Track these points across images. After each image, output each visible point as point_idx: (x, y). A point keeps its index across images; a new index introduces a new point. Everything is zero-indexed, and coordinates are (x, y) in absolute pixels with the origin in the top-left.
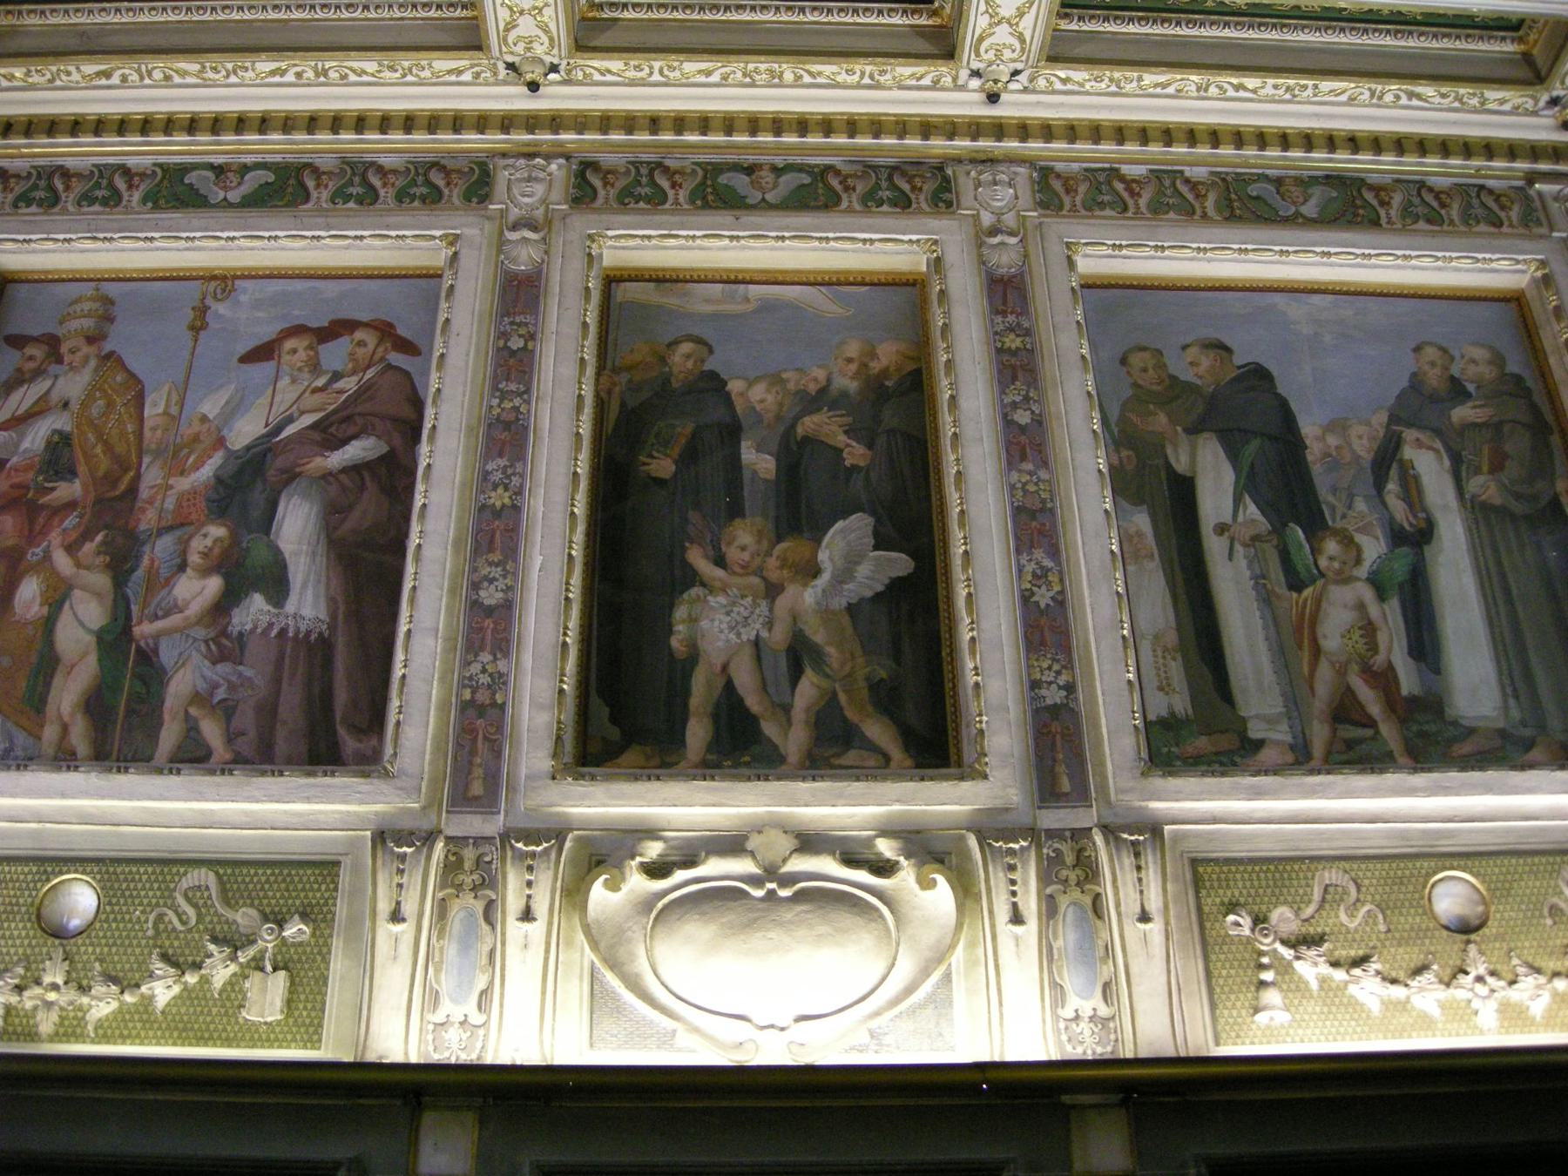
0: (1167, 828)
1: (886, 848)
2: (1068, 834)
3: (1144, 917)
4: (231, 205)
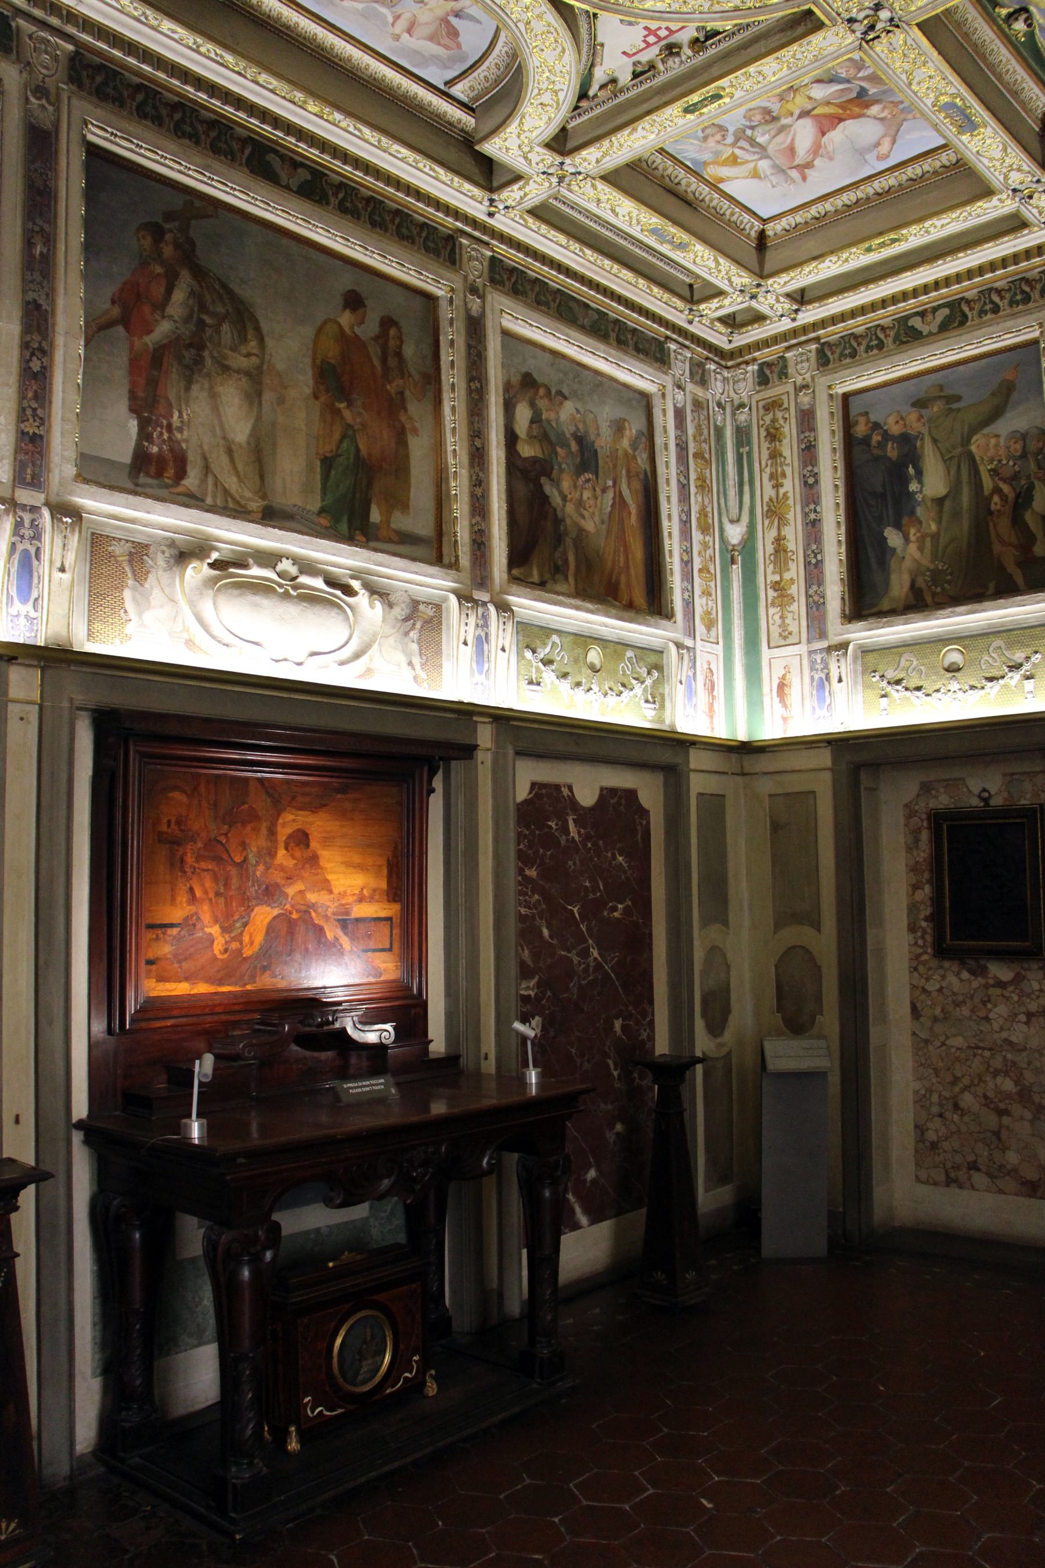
4: (935, 334)
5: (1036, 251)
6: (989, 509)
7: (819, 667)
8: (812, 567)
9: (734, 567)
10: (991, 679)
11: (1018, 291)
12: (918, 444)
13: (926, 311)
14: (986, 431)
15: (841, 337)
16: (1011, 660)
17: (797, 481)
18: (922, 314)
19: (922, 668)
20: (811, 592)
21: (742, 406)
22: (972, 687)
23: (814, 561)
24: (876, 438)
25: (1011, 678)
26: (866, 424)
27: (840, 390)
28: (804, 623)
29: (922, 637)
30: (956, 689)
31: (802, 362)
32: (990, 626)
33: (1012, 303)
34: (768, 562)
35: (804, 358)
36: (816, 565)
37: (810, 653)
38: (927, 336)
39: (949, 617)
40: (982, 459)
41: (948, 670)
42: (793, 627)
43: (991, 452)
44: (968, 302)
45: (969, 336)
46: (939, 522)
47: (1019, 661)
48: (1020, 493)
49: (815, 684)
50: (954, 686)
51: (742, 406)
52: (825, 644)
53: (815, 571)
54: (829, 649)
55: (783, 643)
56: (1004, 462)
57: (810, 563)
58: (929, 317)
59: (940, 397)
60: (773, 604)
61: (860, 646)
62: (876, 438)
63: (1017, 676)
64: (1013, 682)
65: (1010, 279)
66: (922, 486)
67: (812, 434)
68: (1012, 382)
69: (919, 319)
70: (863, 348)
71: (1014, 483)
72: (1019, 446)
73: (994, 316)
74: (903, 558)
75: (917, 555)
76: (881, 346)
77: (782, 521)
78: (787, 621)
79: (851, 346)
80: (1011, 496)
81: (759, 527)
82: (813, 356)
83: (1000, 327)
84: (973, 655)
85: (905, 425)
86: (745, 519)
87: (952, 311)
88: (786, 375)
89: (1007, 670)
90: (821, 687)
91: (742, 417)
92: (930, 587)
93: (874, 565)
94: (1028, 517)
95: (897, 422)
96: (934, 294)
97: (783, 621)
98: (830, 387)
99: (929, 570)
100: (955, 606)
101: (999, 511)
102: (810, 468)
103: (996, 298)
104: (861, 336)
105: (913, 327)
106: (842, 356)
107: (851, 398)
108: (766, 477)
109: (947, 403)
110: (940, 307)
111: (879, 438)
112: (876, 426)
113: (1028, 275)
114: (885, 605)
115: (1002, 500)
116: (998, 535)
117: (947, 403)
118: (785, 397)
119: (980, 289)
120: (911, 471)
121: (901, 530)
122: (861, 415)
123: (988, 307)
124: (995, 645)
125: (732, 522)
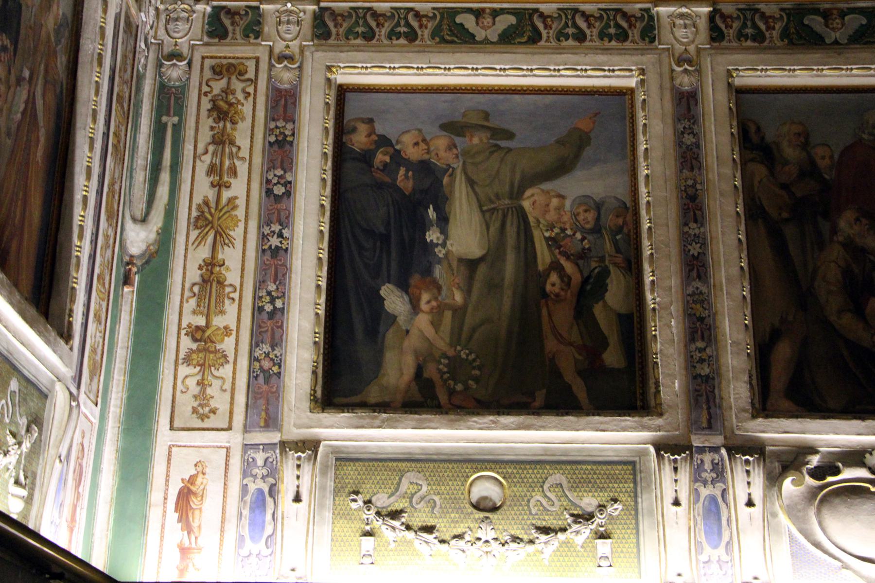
4: (492, 43)
7: (260, 472)
8: (265, 316)
9: (127, 289)
10: (546, 530)
11: (612, 23)
12: (446, 180)
13: (483, 10)
14: (547, 186)
15: (354, 9)
16: (576, 506)
17: (255, 186)
19: (436, 498)
20: (258, 353)
21: (175, 56)
22: (515, 539)
23: (269, 308)
24: (381, 157)
25: (577, 532)
26: (369, 135)
27: (343, 77)
28: (241, 399)
30: (489, 538)
31: (288, 22)
32: (546, 452)
33: (602, 35)
34: (187, 294)
35: (293, 18)
36: (272, 315)
37: (246, 447)
38: (481, 43)
39: (488, 428)
40: (538, 222)
41: (477, 507)
42: (220, 401)
43: (552, 216)
46: (468, 292)
47: (590, 509)
48: (589, 277)
49: (248, 498)
50: (487, 533)
51: (175, 56)
52: (274, 437)
53: (269, 323)
54: (284, 445)
55: (198, 424)
56: (569, 232)
57: (261, 309)
58: (488, 20)
59: (483, 127)
60: (188, 360)
61: (335, 450)
62: (381, 157)
63: (586, 531)
64: (580, 540)
66: (446, 238)
67: (289, 126)
68: (587, 133)
69: (472, 18)
71: (581, 262)
72: (591, 216)
74: (407, 332)
75: (429, 332)
76: (412, 36)
77: (221, 238)
78: (209, 391)
80: (577, 278)
81: (181, 239)
82: (307, 19)
84: (520, 490)
85: (428, 153)
86: (157, 219)
87: (519, 21)
88: (258, 35)
89: (570, 520)
90: (259, 503)
91: (175, 72)
92: (445, 381)
93: (359, 334)
94: (598, 310)
95: (417, 144)
97: (203, 391)
98: (329, 68)
99: (445, 355)
100: (499, 414)
101: (557, 295)
102: (279, 172)
103: (583, 25)
104: (384, 15)
105: (461, 25)
106: (350, 33)
107: (349, 95)
108: (202, 168)
109: (492, 137)
110: (503, 11)
111: (387, 159)
112: (384, 141)
114: (373, 394)
115: (562, 281)
116: (554, 328)
117: (492, 137)
118: (251, 65)
119: (561, 6)
120: (431, 213)
121: (407, 293)
122: (363, 121)
123: (571, 31)
124: (551, 481)
125: (134, 220)
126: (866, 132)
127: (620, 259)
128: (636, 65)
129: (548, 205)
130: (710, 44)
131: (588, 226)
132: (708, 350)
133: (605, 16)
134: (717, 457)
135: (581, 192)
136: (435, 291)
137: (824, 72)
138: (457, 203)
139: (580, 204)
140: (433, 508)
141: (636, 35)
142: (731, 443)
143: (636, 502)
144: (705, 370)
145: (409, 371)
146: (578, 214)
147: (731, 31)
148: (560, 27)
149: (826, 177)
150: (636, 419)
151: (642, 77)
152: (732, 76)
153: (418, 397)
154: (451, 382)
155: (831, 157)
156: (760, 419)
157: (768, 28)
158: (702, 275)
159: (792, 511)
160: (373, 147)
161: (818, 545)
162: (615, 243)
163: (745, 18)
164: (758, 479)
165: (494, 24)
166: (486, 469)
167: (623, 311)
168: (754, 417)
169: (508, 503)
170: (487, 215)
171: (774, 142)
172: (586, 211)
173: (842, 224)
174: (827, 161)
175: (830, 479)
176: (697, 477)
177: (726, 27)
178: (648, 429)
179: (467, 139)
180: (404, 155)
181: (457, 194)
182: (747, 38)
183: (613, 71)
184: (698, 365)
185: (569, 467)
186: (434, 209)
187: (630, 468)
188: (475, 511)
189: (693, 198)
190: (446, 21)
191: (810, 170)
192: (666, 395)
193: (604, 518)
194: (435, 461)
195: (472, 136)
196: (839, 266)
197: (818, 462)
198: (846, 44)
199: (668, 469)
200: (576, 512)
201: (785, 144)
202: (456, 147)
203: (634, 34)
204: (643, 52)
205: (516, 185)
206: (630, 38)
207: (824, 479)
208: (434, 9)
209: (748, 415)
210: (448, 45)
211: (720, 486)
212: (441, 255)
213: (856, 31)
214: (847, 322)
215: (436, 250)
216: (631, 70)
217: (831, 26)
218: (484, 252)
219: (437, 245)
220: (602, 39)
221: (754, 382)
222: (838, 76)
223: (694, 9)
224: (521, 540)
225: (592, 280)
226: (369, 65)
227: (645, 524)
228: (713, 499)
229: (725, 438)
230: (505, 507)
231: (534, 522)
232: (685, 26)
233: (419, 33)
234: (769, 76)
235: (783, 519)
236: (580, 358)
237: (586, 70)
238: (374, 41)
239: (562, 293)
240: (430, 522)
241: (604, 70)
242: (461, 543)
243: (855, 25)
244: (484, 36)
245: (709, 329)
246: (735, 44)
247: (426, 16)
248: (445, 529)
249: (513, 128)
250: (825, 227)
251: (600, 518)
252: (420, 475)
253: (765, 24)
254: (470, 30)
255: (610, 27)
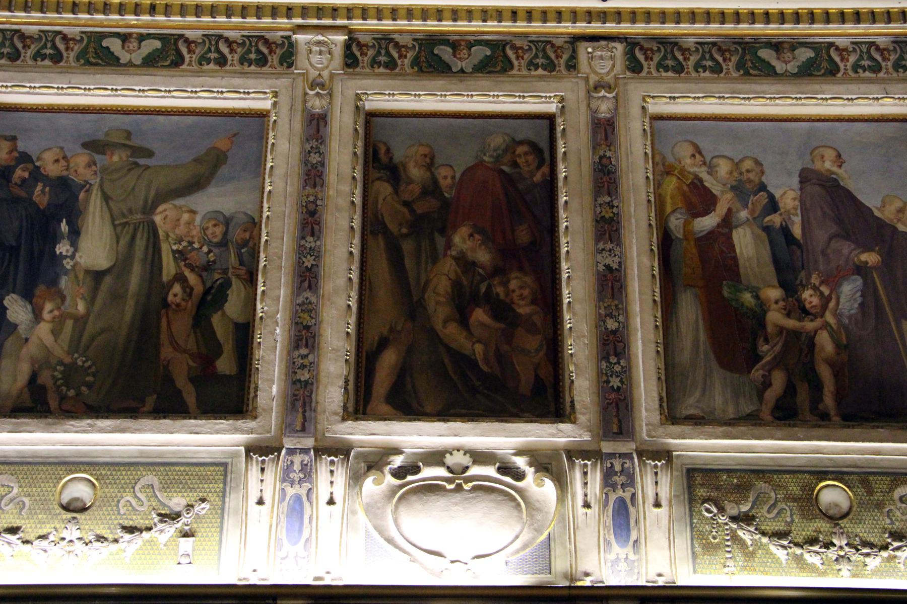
0: (674, 453)
1: (521, 462)
2: (618, 455)
3: (657, 505)
4: (135, 66)
5: (284, 10)
6: (165, 299)
10: (131, 530)
11: (253, 49)
12: (82, 195)
13: (130, 35)
14: (180, 202)
16: (164, 505)
18: (125, 38)
22: (100, 538)
24: (20, 173)
25: (161, 531)
26: (11, 152)
29: (35, 455)
30: (74, 538)
32: (142, 454)
33: (243, 60)
38: (125, 65)
39: (85, 432)
40: (168, 236)
41: (66, 508)
43: (181, 230)
44: (188, 42)
45: (183, 80)
46: (91, 301)
47: (177, 509)
48: (211, 288)
50: (72, 533)
56: (196, 246)
58: (133, 44)
59: (124, 145)
62: (20, 173)
63: (171, 530)
65: (246, 33)
66: (76, 250)
69: (118, 42)
70: (30, 53)
71: (204, 274)
72: (219, 230)
73: (218, 68)
74: (27, 340)
75: (49, 340)
76: (57, 58)
79: (13, 45)
80: (199, 289)
83: (224, 82)
84: (111, 491)
87: (164, 46)
89: (157, 519)
94: (216, 320)
95: (57, 161)
96: (146, 18)
99: (61, 363)
100: (97, 418)
101: (178, 305)
103: (225, 50)
104: (31, 37)
105: (108, 48)
110: (149, 36)
111: (26, 175)
112: (25, 158)
113: (268, 35)
115: (184, 292)
116: (171, 335)
119: (206, 32)
120: (64, 227)
121: (31, 303)
124: (144, 481)
126: (487, 154)
127: (243, 271)
128: (270, 87)
129: (178, 220)
130: (343, 70)
131: (215, 240)
132: (311, 357)
133: (248, 42)
134: (306, 458)
135: (211, 209)
136: (59, 301)
137: (447, 98)
138: (90, 217)
139: (210, 219)
140: (21, 510)
141: (275, 60)
142: (321, 444)
143: (224, 502)
144: (305, 376)
145: (23, 378)
146: (207, 228)
147: (366, 59)
148: (203, 52)
149: (446, 195)
150: (230, 422)
151: (274, 99)
152: (361, 100)
153: (29, 403)
154: (64, 388)
155: (453, 178)
156: (350, 422)
157: (400, 57)
158: (313, 285)
159: (370, 509)
160: (13, 163)
161: (390, 541)
162: (240, 256)
163: (380, 47)
164: (341, 477)
165: (139, 48)
166: (80, 471)
167: (241, 320)
168: (344, 419)
169: (97, 504)
170: (119, 229)
171: (402, 162)
172: (215, 225)
173: (457, 239)
174: (449, 181)
175: (410, 478)
176: (286, 477)
177: (361, 55)
178: (237, 430)
179: (107, 157)
180: (43, 172)
181: (91, 209)
182: (379, 64)
183: (248, 93)
184: (299, 371)
185: (162, 469)
186: (67, 223)
187: (222, 469)
188: (63, 512)
189: (312, 213)
190: (92, 45)
191: (432, 189)
192: (262, 400)
193: (190, 517)
194: (50, 464)
195: (112, 154)
196: (450, 279)
197: (402, 462)
198: (471, 73)
199: (254, 471)
200: (163, 512)
201: (411, 165)
202: (95, 164)
203: (274, 59)
204: (278, 76)
205: (150, 202)
206: (269, 64)
207: (404, 477)
208: (82, 32)
209: (339, 418)
210: (92, 67)
211: (307, 485)
212: (69, 267)
213: (481, 62)
214: (452, 333)
215: (64, 262)
216: (265, 93)
217: (458, 56)
218: (112, 263)
219: (66, 257)
220: (242, 64)
221: (351, 387)
222: (461, 102)
223: (329, 37)
224: (106, 539)
225: (213, 291)
226: (9, 84)
227: (230, 523)
228: (298, 498)
229: (316, 440)
230: (94, 508)
231: (121, 522)
232: (320, 53)
233: (65, 55)
234: (397, 101)
235: (361, 516)
236: (195, 365)
237: (222, 92)
238: (19, 62)
239: (183, 303)
240: (16, 523)
241: (240, 92)
242: (45, 543)
243: (481, 57)
244: (128, 60)
245: (314, 337)
246: (368, 70)
247: (73, 39)
248: (30, 529)
249: (155, 146)
250: (440, 241)
251: (186, 518)
252: (13, 478)
253: (398, 52)
254: (116, 54)
255: (251, 53)
